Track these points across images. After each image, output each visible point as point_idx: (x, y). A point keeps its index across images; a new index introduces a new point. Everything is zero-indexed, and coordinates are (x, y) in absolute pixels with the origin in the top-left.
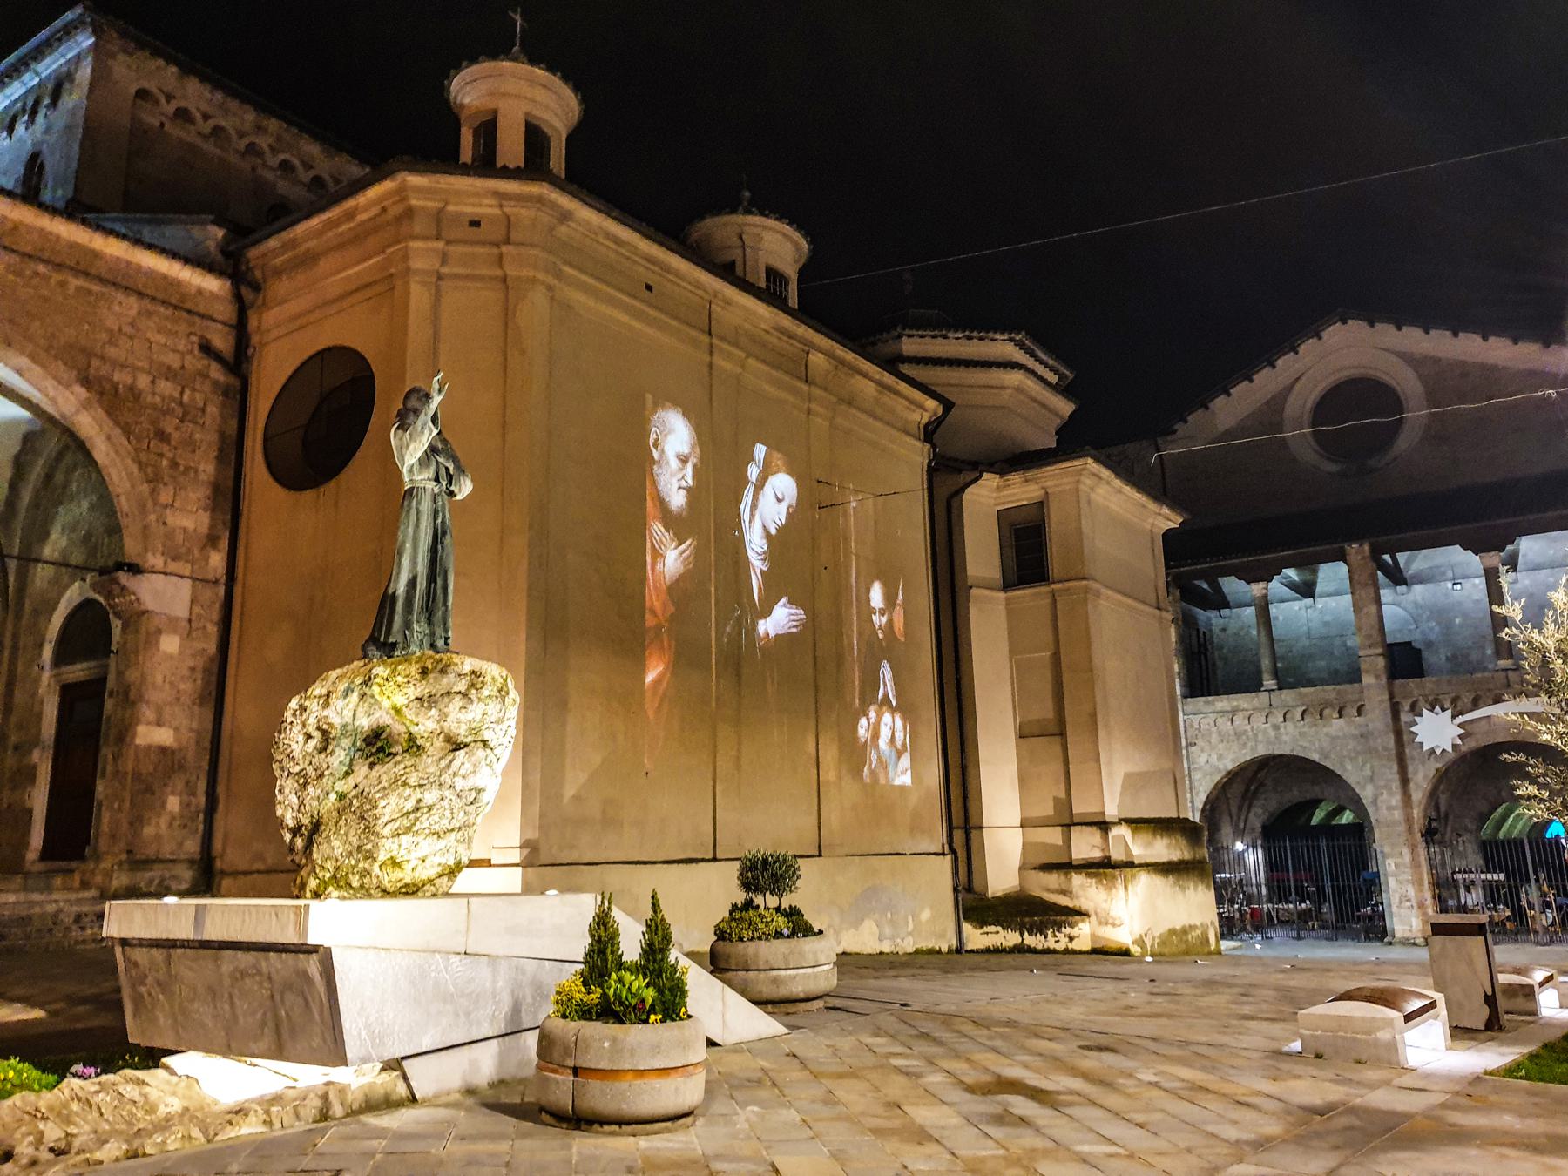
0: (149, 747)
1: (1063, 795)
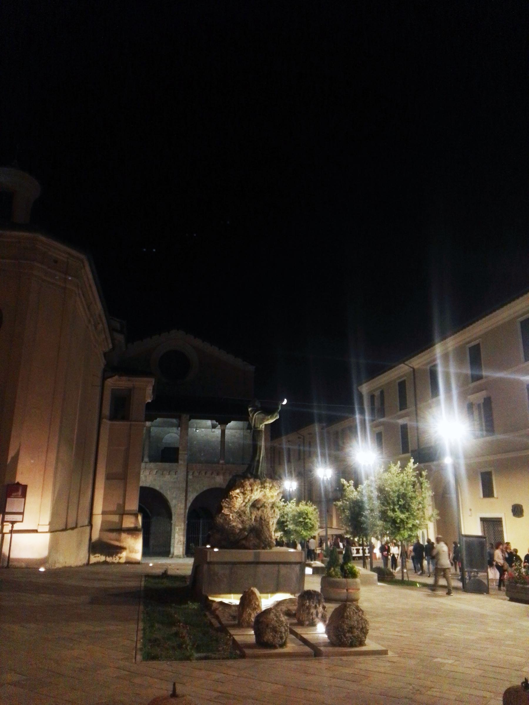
1: (121, 502)
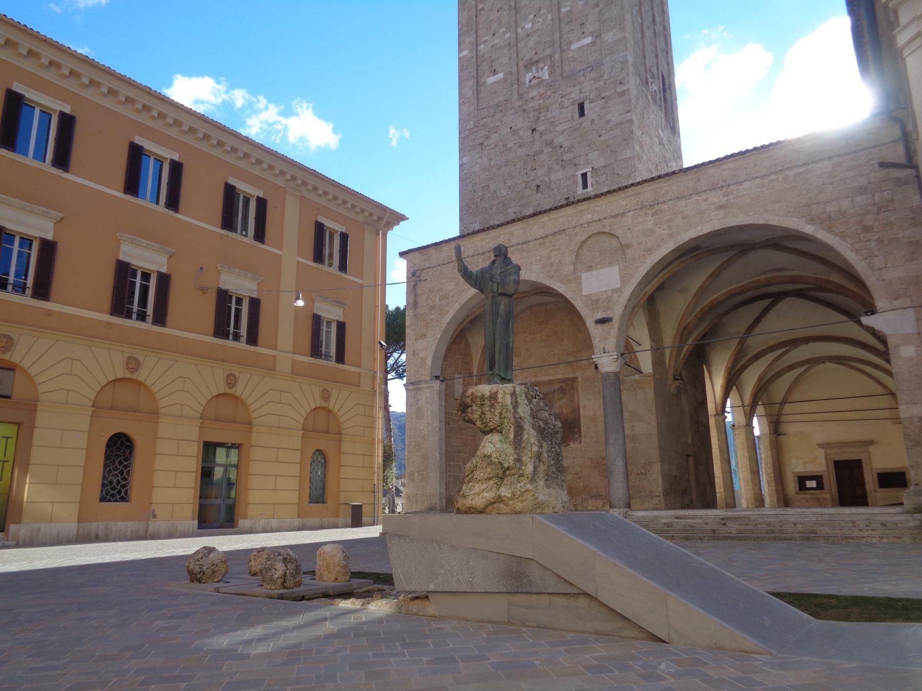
0: (911, 418)
